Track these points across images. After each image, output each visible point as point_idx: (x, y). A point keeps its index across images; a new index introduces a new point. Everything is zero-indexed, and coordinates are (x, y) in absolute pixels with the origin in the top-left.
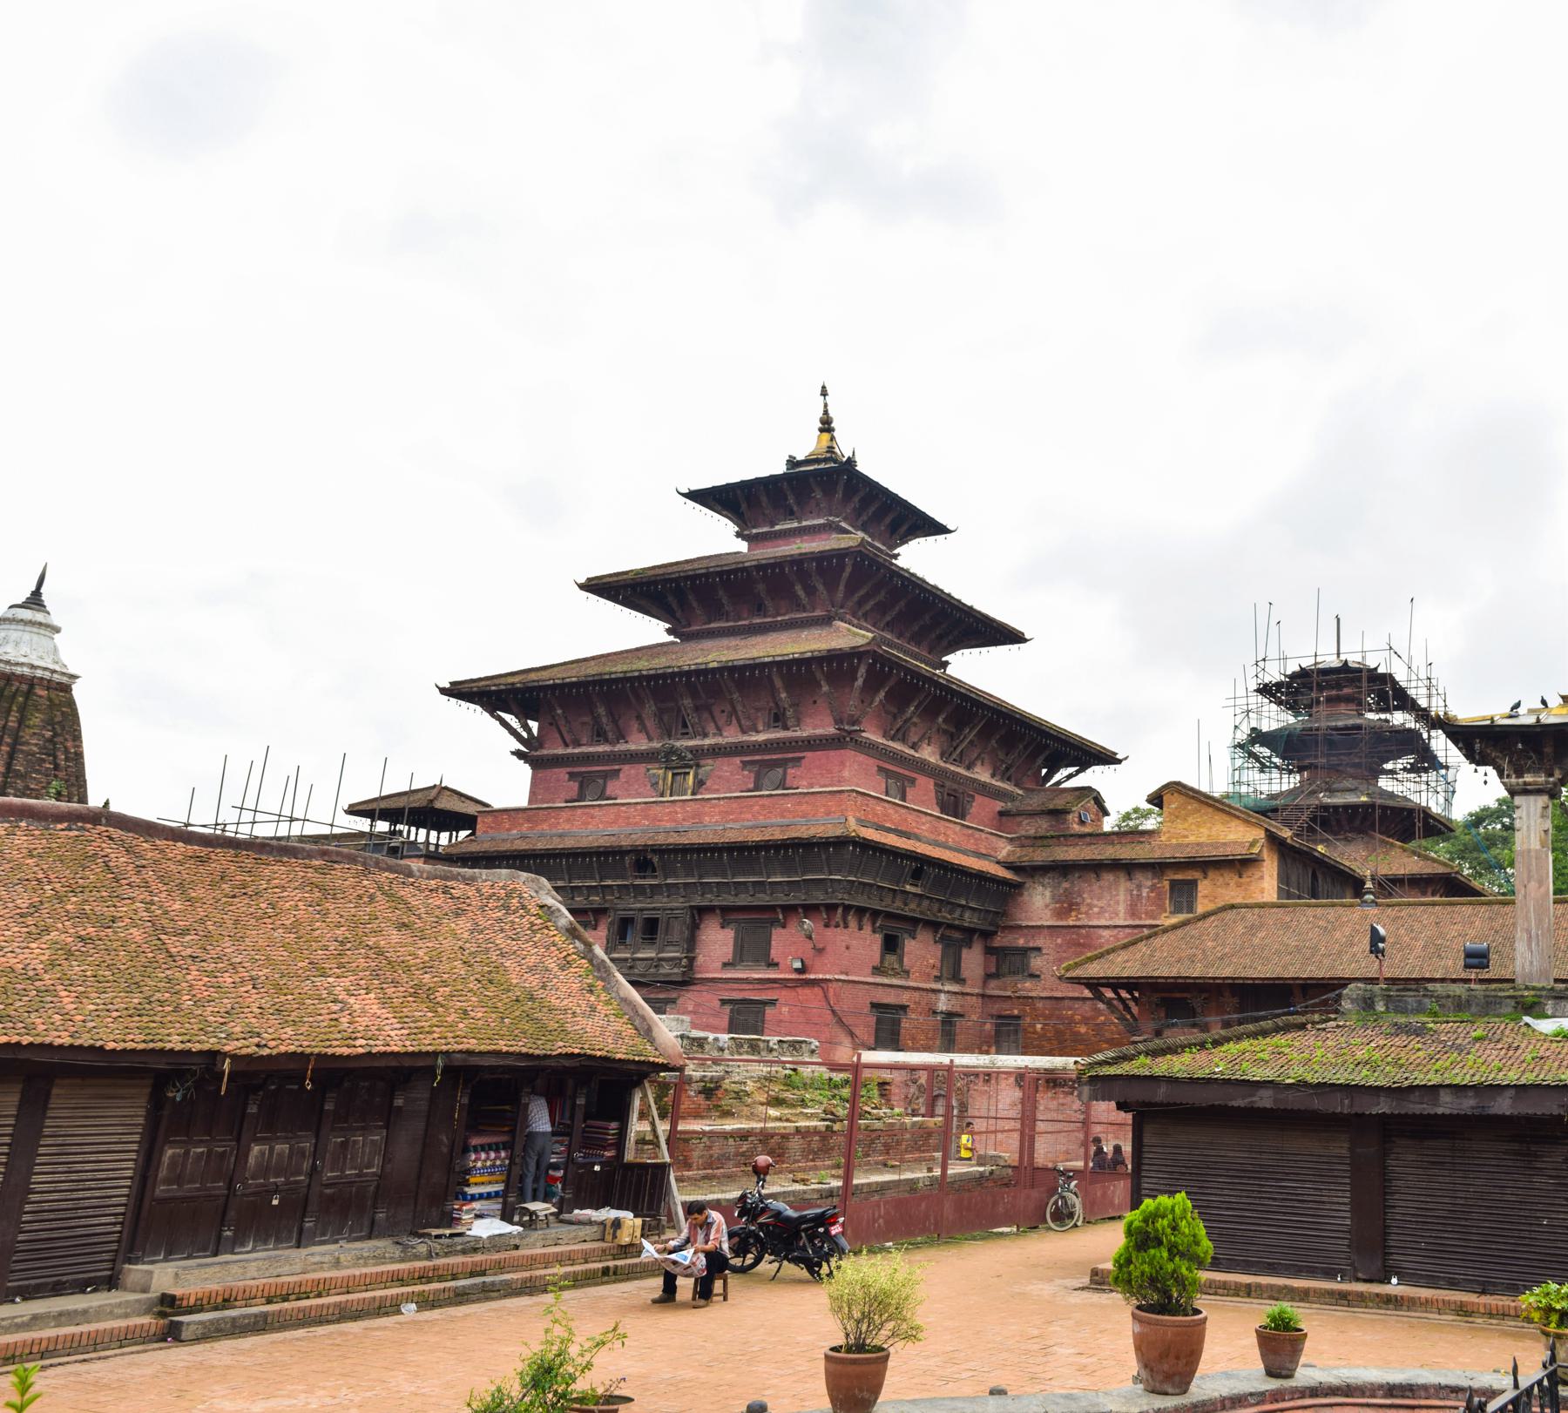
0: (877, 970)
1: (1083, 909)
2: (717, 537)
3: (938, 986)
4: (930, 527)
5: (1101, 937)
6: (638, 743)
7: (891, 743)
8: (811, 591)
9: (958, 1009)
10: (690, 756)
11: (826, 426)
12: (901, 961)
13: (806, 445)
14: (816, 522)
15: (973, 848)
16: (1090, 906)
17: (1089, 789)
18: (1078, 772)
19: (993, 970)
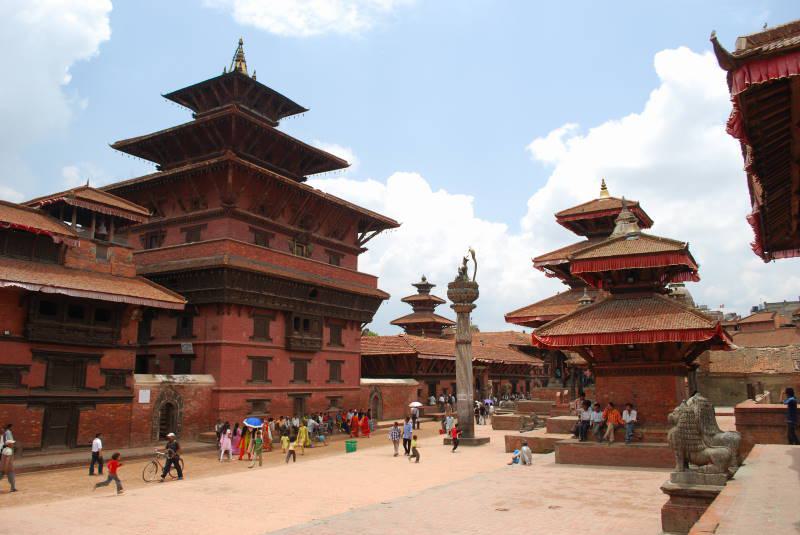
4: (293, 108)
11: (240, 57)
13: (230, 68)
18: (378, 232)
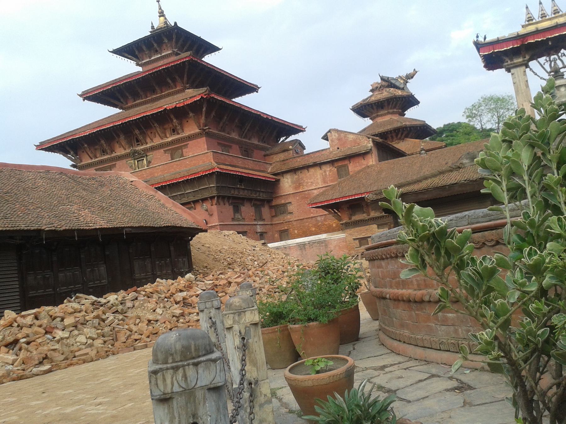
0: (233, 219)
1: (305, 184)
2: (128, 68)
3: (256, 223)
5: (313, 193)
6: (120, 151)
7: (220, 133)
8: (174, 81)
9: (264, 231)
10: (143, 152)
11: (162, 14)
12: (241, 215)
14: (167, 53)
15: (258, 168)
16: (307, 183)
17: (297, 140)
19: (274, 214)
